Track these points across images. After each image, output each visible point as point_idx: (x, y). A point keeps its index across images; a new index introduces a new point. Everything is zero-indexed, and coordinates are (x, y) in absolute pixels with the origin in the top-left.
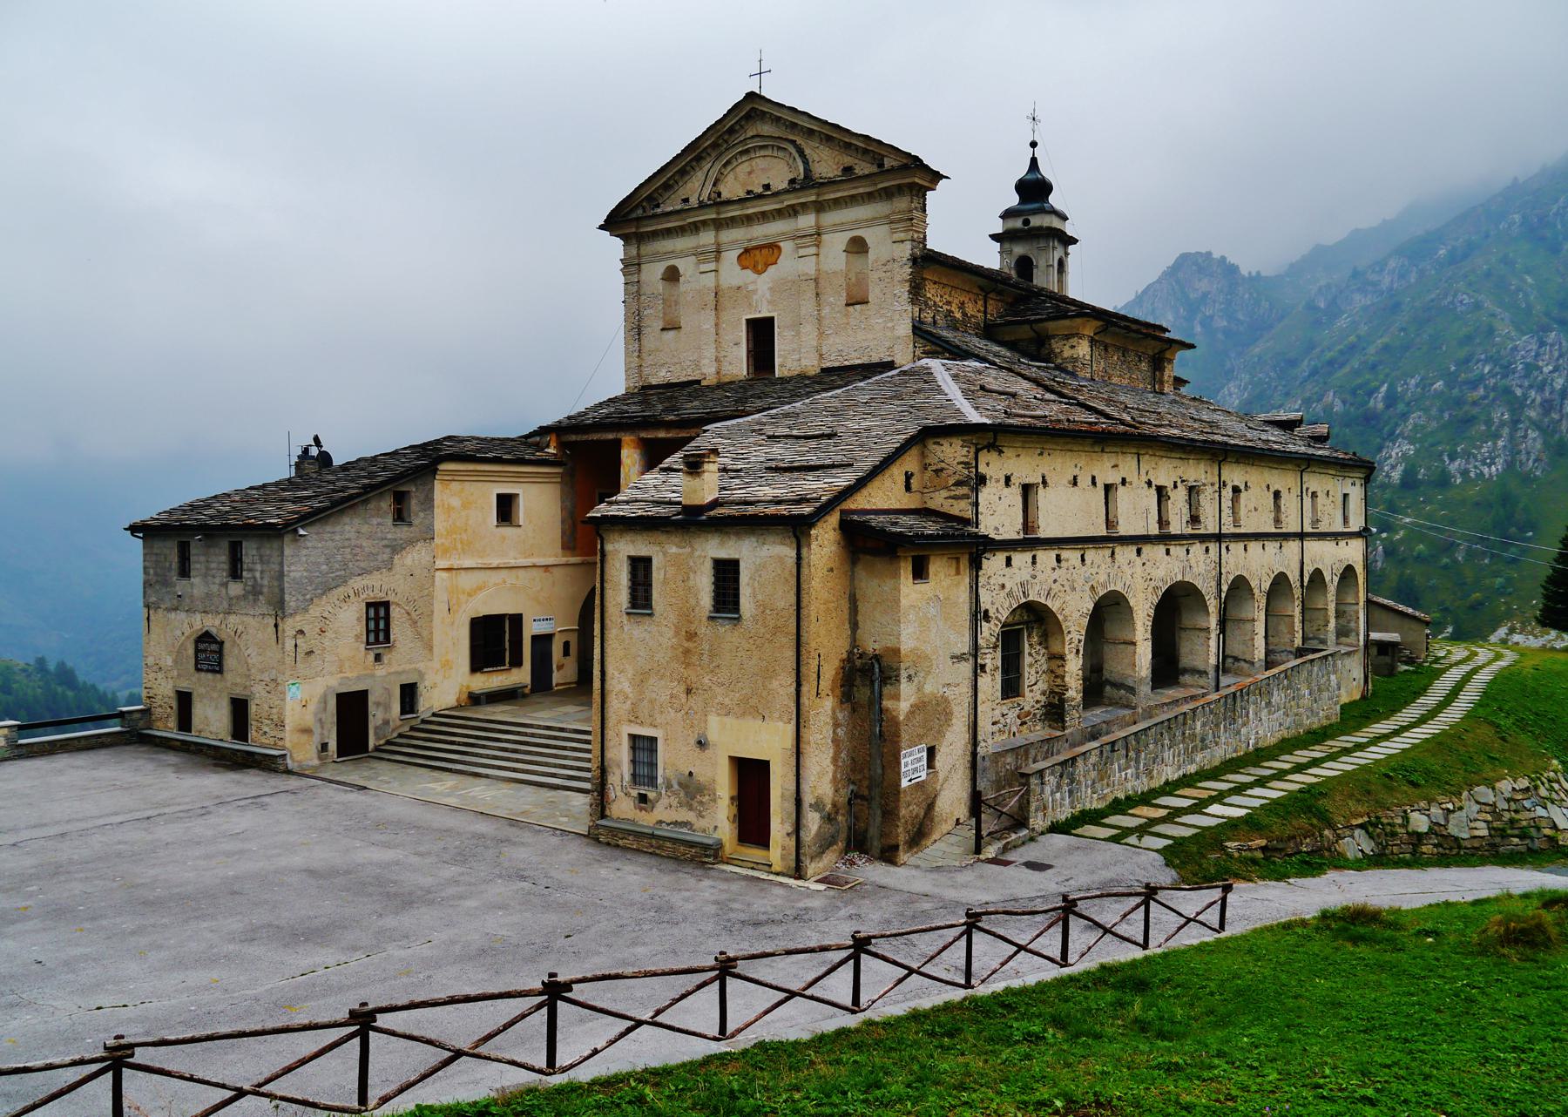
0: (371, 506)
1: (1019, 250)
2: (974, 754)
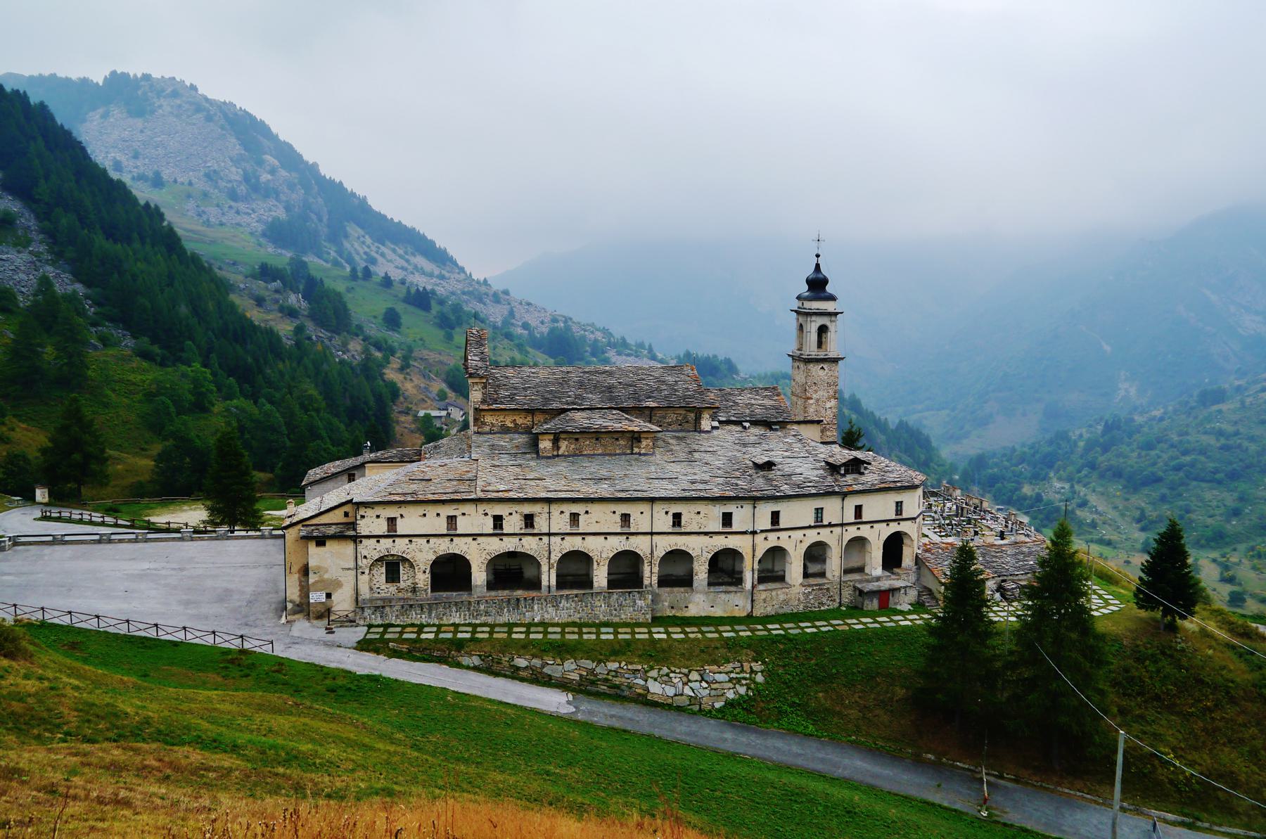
0: (339, 478)
1: (801, 319)
2: (357, 598)
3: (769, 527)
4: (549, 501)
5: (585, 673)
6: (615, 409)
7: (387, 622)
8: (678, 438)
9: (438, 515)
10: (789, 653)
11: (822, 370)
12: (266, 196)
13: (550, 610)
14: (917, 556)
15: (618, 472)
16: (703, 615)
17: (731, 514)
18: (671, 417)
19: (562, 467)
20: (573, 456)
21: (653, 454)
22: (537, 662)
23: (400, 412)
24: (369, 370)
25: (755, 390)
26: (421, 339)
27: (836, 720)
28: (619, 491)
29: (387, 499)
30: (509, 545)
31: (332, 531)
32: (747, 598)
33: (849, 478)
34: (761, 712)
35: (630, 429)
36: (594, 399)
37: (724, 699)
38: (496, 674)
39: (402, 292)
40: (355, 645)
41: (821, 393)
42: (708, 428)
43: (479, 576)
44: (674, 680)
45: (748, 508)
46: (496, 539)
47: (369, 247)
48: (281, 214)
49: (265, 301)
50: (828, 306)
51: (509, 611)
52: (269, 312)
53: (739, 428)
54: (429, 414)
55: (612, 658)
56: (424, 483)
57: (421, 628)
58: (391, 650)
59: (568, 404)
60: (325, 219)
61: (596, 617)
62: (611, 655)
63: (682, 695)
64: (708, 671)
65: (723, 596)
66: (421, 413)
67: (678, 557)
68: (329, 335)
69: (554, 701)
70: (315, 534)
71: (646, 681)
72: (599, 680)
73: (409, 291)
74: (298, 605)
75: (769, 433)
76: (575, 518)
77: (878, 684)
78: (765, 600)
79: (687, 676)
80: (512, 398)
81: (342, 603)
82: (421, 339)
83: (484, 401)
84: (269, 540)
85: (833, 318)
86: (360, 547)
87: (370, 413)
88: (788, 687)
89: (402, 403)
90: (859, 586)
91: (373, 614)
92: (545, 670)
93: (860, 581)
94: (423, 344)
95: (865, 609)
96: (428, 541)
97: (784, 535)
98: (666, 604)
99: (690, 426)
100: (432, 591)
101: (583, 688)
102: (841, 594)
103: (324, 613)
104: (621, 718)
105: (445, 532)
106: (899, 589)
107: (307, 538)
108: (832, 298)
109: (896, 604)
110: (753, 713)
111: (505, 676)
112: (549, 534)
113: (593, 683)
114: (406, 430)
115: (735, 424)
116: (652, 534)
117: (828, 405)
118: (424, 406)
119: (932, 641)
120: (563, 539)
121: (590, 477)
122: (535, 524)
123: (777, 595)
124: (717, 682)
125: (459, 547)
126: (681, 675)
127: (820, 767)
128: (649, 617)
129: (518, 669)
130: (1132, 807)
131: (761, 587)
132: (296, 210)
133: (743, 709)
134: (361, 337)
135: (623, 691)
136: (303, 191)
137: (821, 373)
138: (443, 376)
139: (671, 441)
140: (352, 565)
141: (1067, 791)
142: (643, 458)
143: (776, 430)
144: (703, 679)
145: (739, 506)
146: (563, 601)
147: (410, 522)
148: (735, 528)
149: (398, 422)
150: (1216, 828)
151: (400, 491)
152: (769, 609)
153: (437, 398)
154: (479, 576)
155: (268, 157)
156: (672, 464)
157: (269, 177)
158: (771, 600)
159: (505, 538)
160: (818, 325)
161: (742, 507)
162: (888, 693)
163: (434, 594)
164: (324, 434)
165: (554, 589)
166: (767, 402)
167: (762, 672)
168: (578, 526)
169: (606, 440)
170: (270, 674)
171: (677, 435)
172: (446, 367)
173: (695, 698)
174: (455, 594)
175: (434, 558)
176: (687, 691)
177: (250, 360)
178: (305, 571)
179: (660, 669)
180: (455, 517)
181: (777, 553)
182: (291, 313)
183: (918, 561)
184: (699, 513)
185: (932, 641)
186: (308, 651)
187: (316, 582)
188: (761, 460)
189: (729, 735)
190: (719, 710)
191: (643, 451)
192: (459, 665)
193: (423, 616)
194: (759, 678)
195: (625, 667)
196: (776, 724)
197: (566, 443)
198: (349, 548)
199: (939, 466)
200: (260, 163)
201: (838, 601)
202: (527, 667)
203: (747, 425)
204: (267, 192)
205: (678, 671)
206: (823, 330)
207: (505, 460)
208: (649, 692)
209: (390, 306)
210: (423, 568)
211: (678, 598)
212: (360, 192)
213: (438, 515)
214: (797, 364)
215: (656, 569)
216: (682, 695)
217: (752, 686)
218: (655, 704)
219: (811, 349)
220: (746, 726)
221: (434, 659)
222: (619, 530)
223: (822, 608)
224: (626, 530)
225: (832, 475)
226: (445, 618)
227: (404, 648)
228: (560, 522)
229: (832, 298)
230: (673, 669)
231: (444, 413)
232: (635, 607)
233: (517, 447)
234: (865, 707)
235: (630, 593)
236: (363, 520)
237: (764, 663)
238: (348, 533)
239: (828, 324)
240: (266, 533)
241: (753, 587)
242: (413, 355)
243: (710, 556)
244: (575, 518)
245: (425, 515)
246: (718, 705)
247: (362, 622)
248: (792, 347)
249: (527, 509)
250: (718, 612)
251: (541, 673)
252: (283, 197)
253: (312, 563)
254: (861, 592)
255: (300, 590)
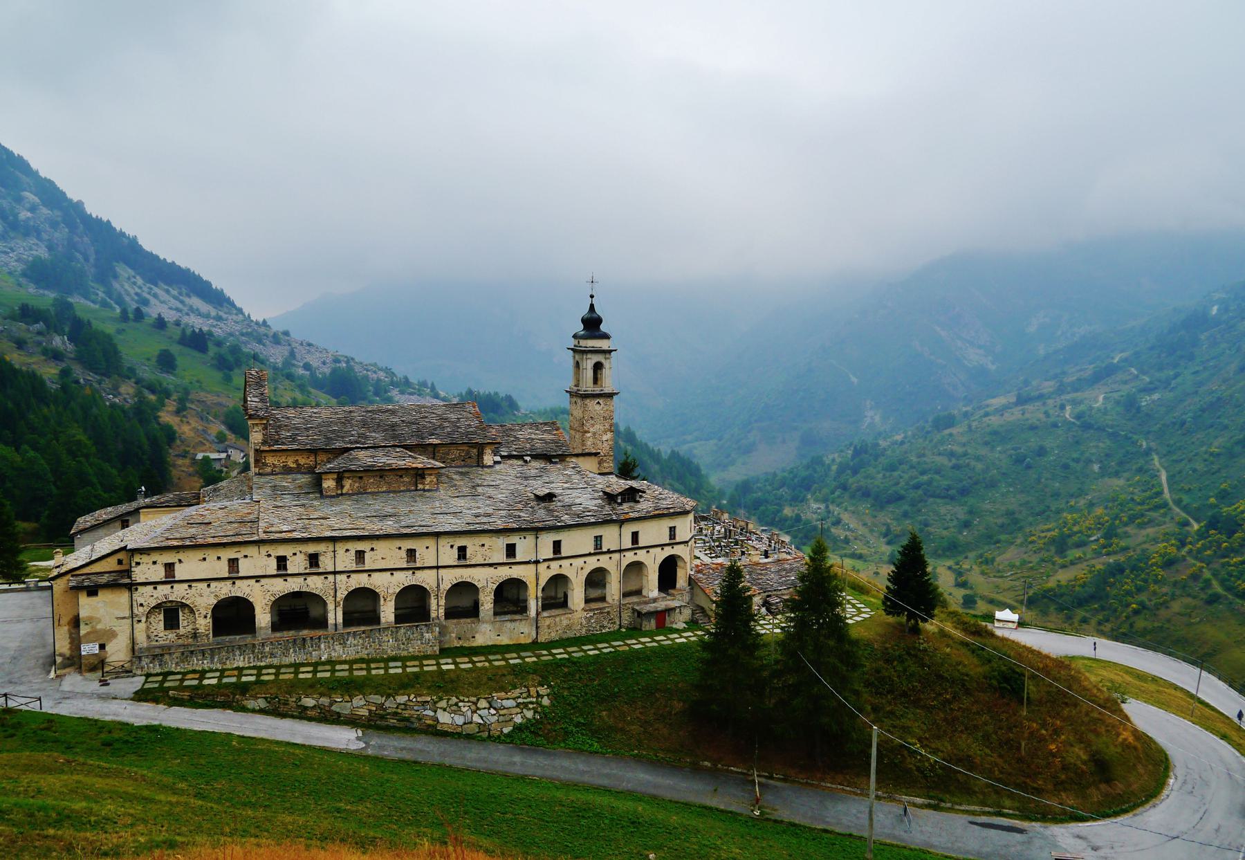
1: (577, 357)
2: (133, 648)
3: (551, 556)
4: (333, 540)
5: (374, 709)
6: (399, 446)
7: (166, 670)
8: (461, 474)
9: (219, 558)
10: (573, 675)
11: (598, 405)
12: (26, 234)
13: (337, 648)
14: (690, 578)
15: (403, 509)
16: (490, 643)
17: (514, 545)
18: (455, 453)
19: (347, 505)
20: (357, 494)
21: (436, 490)
22: (325, 701)
23: (177, 456)
24: (143, 413)
25: (535, 425)
26: (198, 381)
27: (619, 736)
28: (405, 527)
29: (164, 544)
30: (294, 585)
31: (104, 579)
32: (532, 626)
33: (626, 506)
34: (548, 734)
35: (414, 466)
36: (377, 437)
37: (512, 724)
38: (283, 716)
39: (177, 333)
40: (133, 695)
41: (597, 427)
42: (490, 463)
43: (263, 618)
44: (464, 709)
45: (530, 539)
46: (280, 580)
47: (140, 288)
48: (42, 253)
49: (25, 342)
50: (603, 344)
51: (295, 651)
52: (31, 355)
53: (520, 462)
54: (208, 457)
55: (401, 692)
56: (203, 526)
57: (202, 674)
58: (170, 698)
59: (351, 443)
60: (92, 260)
61: (385, 651)
62: (400, 689)
63: (471, 723)
64: (495, 698)
65: (509, 625)
66: (200, 456)
67: (464, 589)
68: (98, 378)
69: (344, 738)
70: (86, 584)
71: (435, 712)
72: (389, 714)
73: (184, 331)
74: (68, 659)
75: (549, 466)
76: (360, 555)
77: (657, 700)
78: (549, 627)
79: (475, 704)
80: (293, 439)
81: (117, 652)
82: (198, 381)
83: (264, 442)
84: (36, 594)
85: (607, 356)
86: (135, 595)
87: (145, 457)
88: (573, 708)
89: (178, 446)
90: (637, 608)
91: (151, 663)
92: (333, 708)
93: (638, 604)
94: (200, 387)
95: (643, 629)
96: (209, 586)
97: (565, 563)
98: (454, 635)
99: (473, 462)
100: (214, 636)
101: (373, 724)
102: (620, 617)
103: (98, 665)
104: (411, 750)
105: (227, 575)
106: (674, 609)
107: (77, 589)
108: (606, 336)
109: (672, 623)
110: (540, 736)
111: (293, 717)
112: (335, 573)
113: (382, 717)
114: (184, 474)
115: (516, 459)
116: (438, 567)
117: (605, 438)
118: (202, 449)
119: (706, 655)
120: (349, 577)
121: (375, 514)
122: (320, 563)
123: (561, 620)
124: (505, 708)
125: (242, 589)
126: (470, 704)
127: (605, 782)
128: (437, 649)
129: (306, 708)
130: (885, 795)
131: (545, 614)
132: (60, 249)
133: (532, 732)
134: (133, 380)
135: (412, 723)
136: (67, 230)
137: (597, 407)
138: (222, 418)
139: (454, 477)
140: (127, 613)
141: (829, 785)
142: (428, 494)
143: (556, 463)
144: (491, 706)
145: (522, 537)
146: (350, 638)
147: (189, 566)
148: (519, 558)
149: (174, 466)
150: (957, 807)
151: (178, 536)
152: (553, 634)
153: (216, 440)
154: (263, 618)
155: (27, 194)
156: (456, 499)
157: (29, 215)
158: (555, 625)
159: (289, 579)
160: (594, 361)
161: (525, 538)
162: (666, 706)
163: (216, 638)
164: (94, 480)
165: (340, 627)
166: (546, 436)
167: (548, 695)
168: (364, 563)
169: (391, 478)
170: (39, 732)
171: (460, 470)
172: (225, 409)
173: (484, 725)
174: (238, 637)
175: (215, 602)
176: (476, 719)
177: (10, 405)
178: (76, 622)
179: (449, 699)
180: (237, 559)
181: (559, 581)
182: (56, 356)
183: (691, 581)
184: (483, 545)
185: (706, 655)
186: (81, 705)
187: (88, 633)
188: (543, 491)
189: (517, 759)
190: (509, 735)
191: (427, 487)
192: (244, 709)
193: (205, 662)
194: (546, 701)
195: (414, 700)
196: (562, 745)
197: (350, 481)
198: (123, 597)
199: (708, 492)
200: (19, 200)
201: (618, 623)
202: (315, 706)
203: (528, 458)
204: (27, 231)
205: (466, 700)
206: (598, 367)
207: (288, 500)
208: (438, 722)
209: (166, 348)
210: (204, 613)
211: (465, 629)
212: (130, 231)
213: (219, 558)
214: (574, 399)
215: (442, 602)
216: (471, 723)
217: (539, 709)
218: (444, 734)
219: (587, 385)
220: (534, 748)
221: (218, 704)
222: (405, 566)
223: (604, 631)
224: (412, 565)
225: (610, 504)
226: (228, 662)
227: (186, 695)
228: (345, 559)
229: (606, 336)
230: (462, 698)
231: (223, 455)
232: (424, 640)
233: (299, 487)
234: (646, 722)
235: (417, 626)
236: (139, 567)
237: (549, 686)
238: (122, 581)
239: (603, 361)
240: (32, 585)
241: (538, 614)
242: (190, 397)
243: (495, 587)
244: (360, 555)
245: (204, 559)
246: (506, 731)
247: (139, 672)
248: (569, 384)
249: (312, 549)
250: (504, 640)
251: (329, 711)
252: (45, 236)
253: (83, 614)
254: (639, 614)
255: (70, 643)
